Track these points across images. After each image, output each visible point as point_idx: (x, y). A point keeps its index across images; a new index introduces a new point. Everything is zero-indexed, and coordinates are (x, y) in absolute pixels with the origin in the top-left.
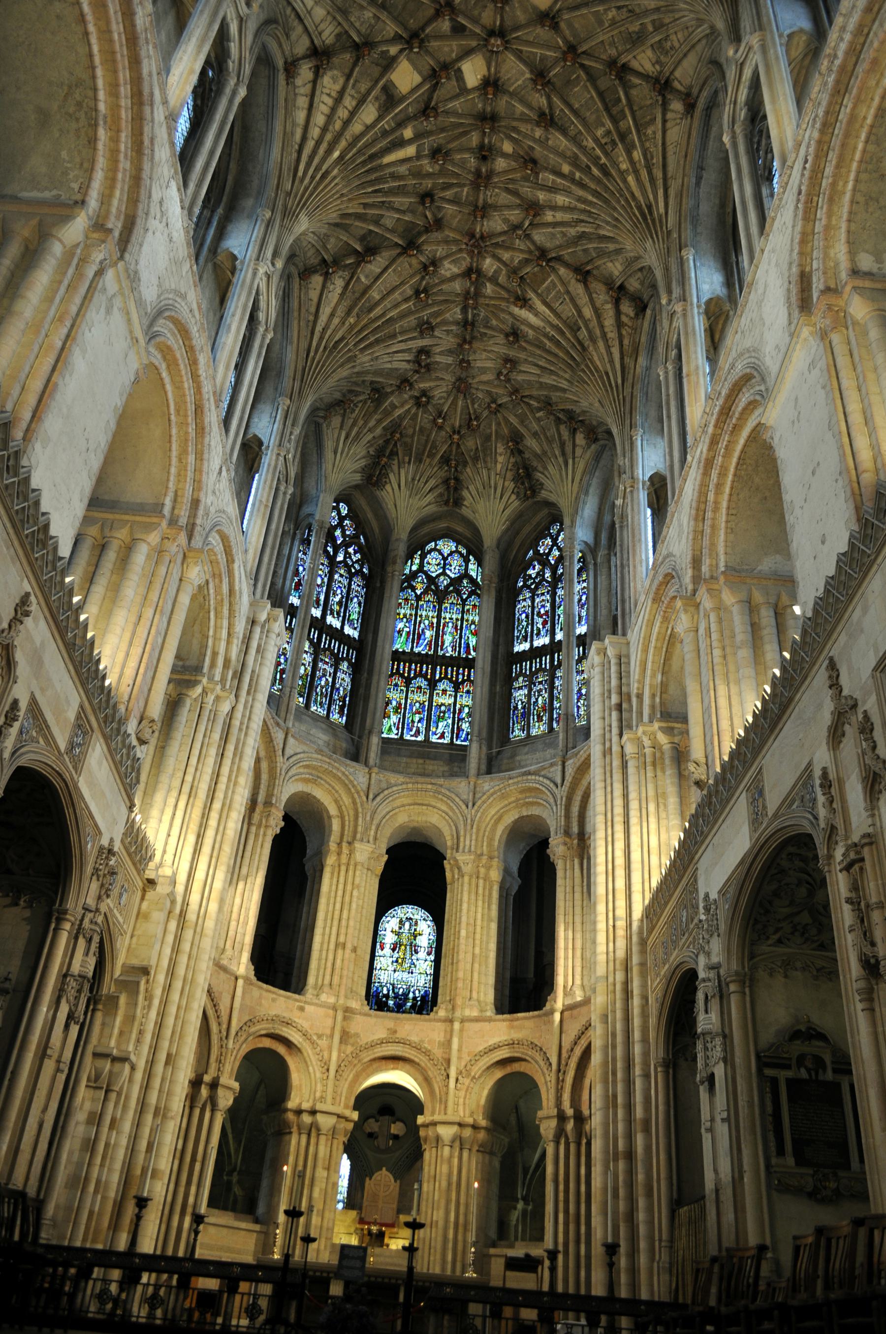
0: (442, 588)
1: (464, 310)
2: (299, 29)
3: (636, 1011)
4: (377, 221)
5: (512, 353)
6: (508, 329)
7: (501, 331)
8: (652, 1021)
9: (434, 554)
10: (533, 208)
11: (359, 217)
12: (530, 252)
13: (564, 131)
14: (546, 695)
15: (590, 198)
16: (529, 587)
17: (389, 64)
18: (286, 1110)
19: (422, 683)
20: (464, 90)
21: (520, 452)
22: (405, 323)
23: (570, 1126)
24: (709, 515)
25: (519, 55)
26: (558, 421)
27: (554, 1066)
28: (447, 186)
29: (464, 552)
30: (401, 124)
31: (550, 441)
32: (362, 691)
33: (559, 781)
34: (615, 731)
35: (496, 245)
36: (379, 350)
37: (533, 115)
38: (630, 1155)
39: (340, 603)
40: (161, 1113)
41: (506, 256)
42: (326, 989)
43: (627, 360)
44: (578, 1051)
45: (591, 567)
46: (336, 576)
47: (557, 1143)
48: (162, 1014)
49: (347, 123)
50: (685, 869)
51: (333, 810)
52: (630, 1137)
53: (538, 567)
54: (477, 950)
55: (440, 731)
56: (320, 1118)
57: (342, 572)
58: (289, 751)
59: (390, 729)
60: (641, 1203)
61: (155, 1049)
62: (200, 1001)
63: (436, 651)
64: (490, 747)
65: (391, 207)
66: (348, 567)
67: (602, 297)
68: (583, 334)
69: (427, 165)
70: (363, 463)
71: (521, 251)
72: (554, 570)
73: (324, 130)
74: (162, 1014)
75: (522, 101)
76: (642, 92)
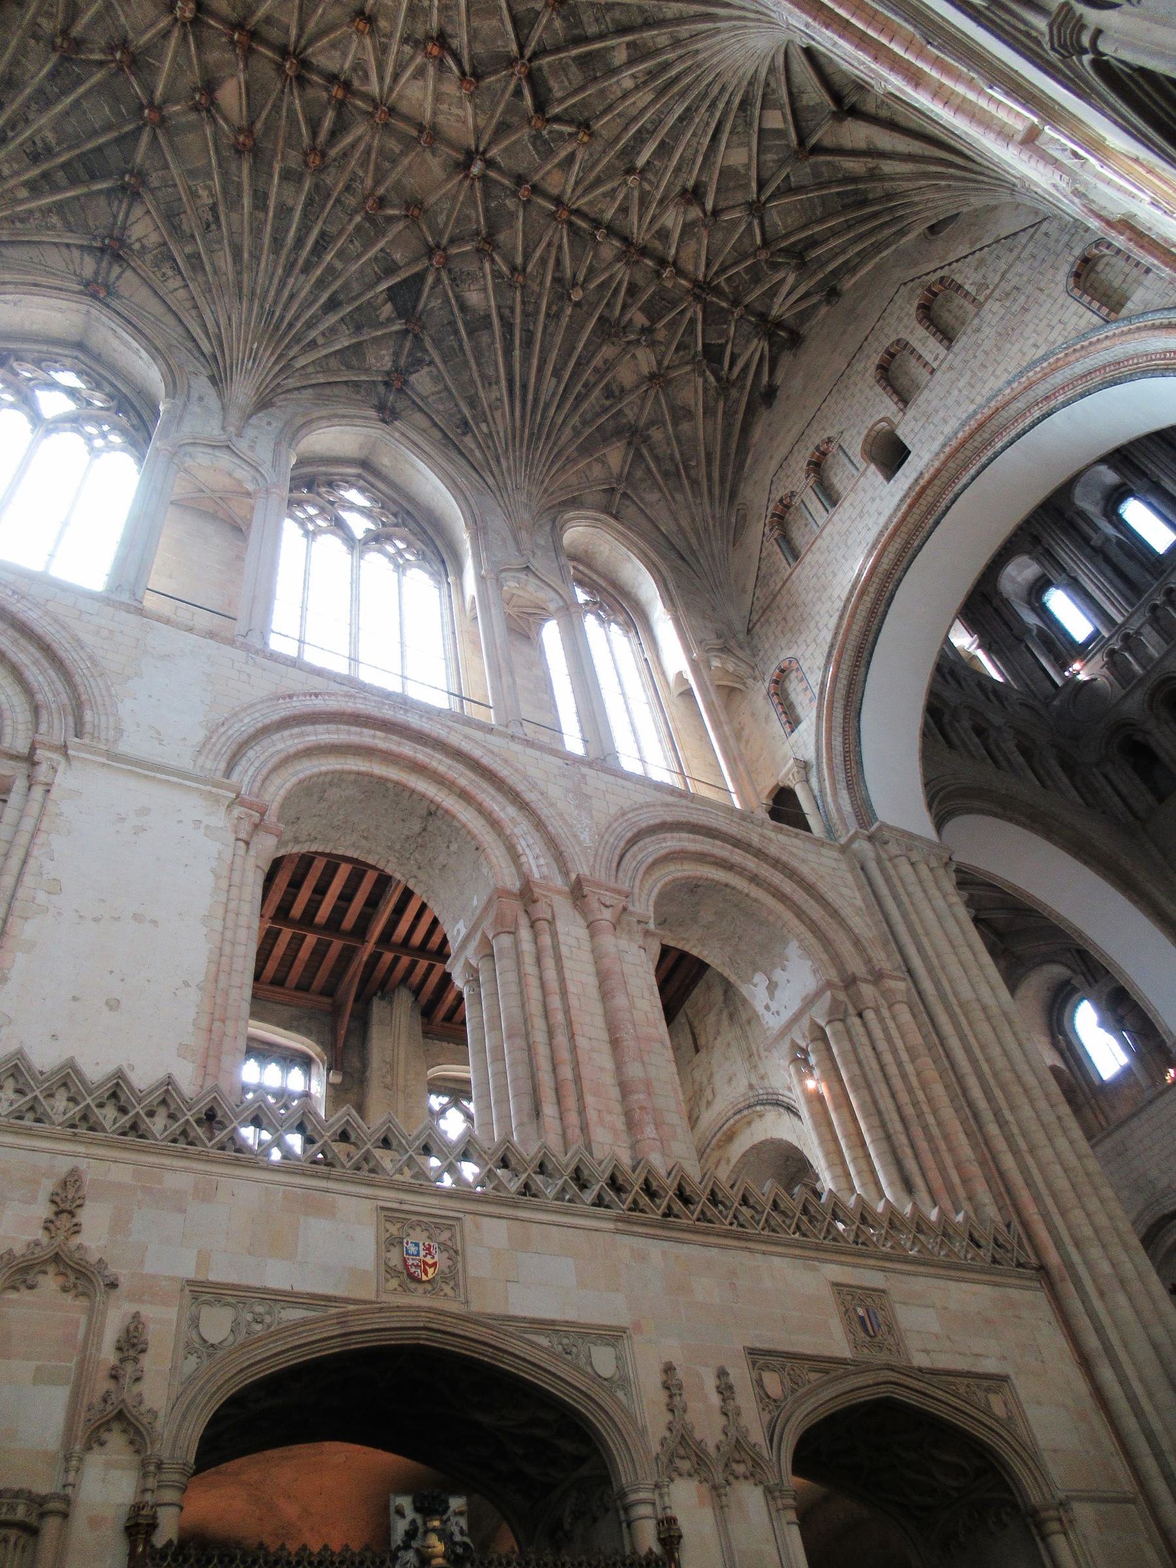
13: (53, 75)
25: (165, 35)
75: (99, 18)
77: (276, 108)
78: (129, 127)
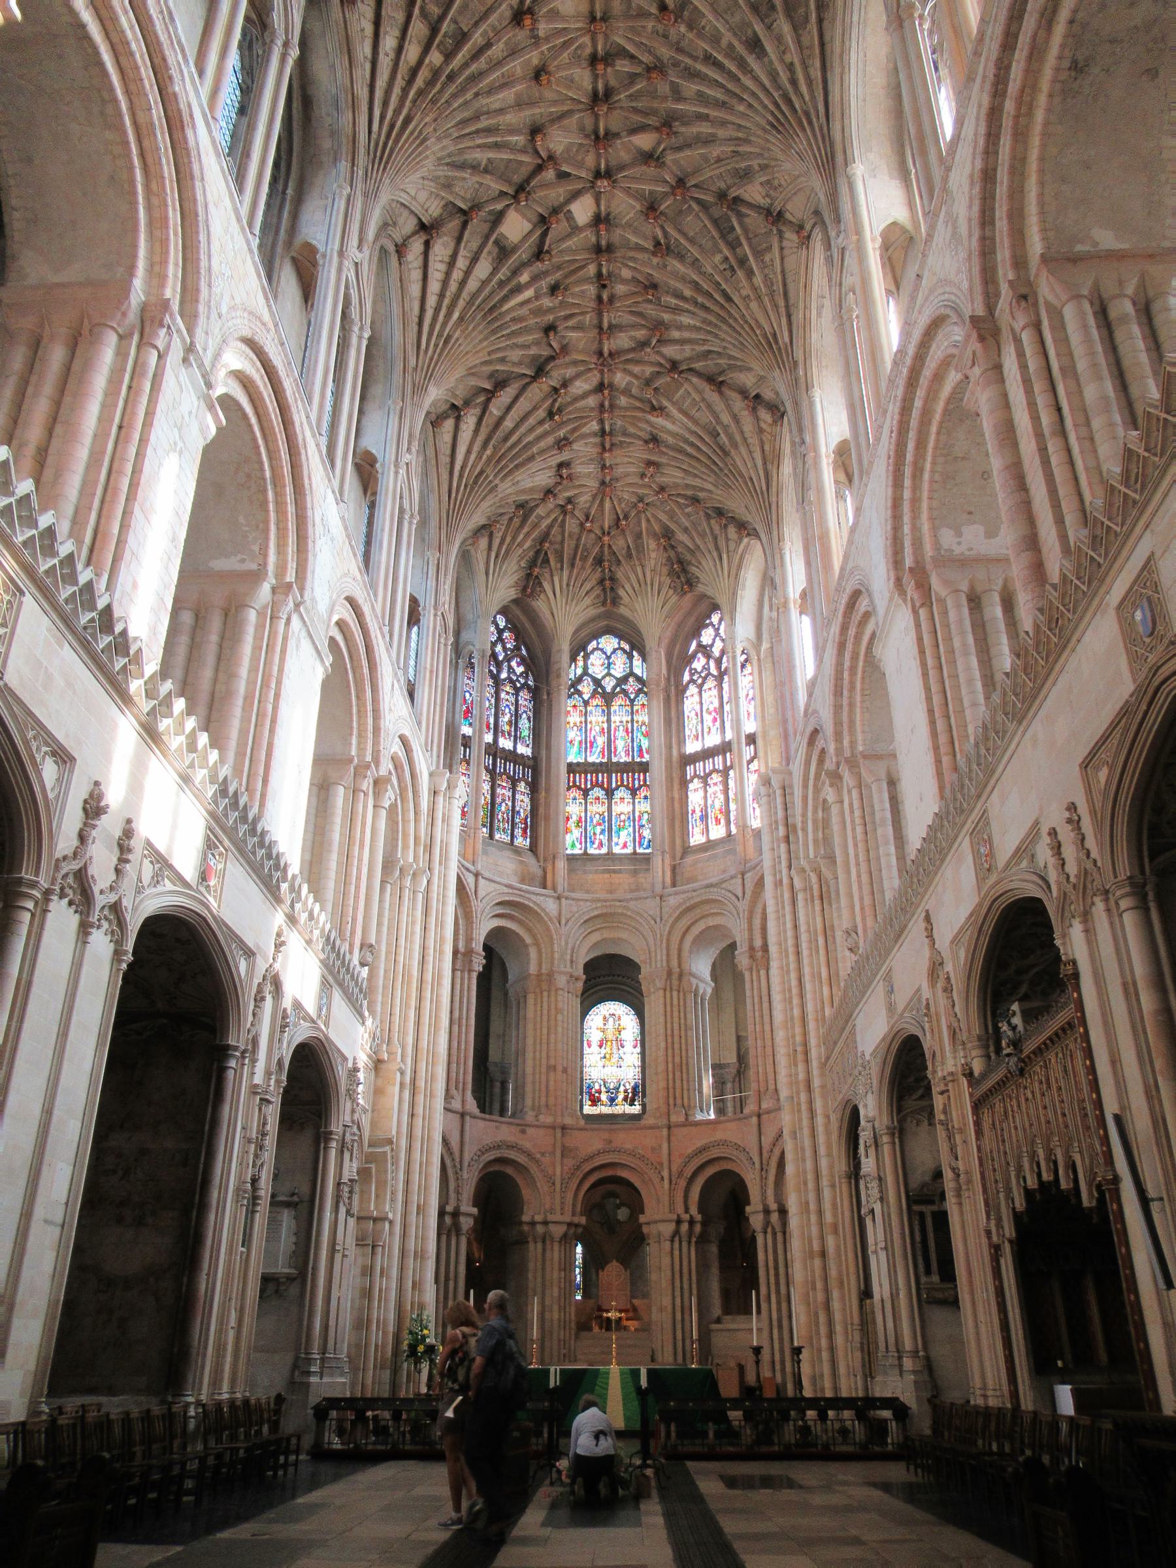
0: (609, 689)
1: (601, 421)
2: (406, 213)
3: (820, 1129)
4: (503, 360)
5: (654, 458)
6: (647, 437)
7: (639, 438)
8: (835, 1137)
9: (597, 654)
10: (658, 326)
11: (486, 363)
12: (661, 365)
13: (681, 257)
14: (722, 797)
15: (714, 320)
16: (694, 682)
17: (498, 218)
18: (521, 1223)
19: (598, 792)
20: (575, 229)
21: (673, 547)
22: (543, 444)
23: (775, 1218)
24: (845, 693)
25: (627, 190)
26: (708, 517)
27: (757, 1165)
28: (568, 317)
29: (627, 647)
30: (515, 272)
31: (703, 535)
32: (541, 810)
33: (740, 895)
34: (784, 864)
35: (628, 361)
36: (520, 475)
37: (649, 245)
38: (823, 1254)
39: (510, 723)
40: (420, 1255)
41: (637, 369)
42: (543, 1110)
43: (769, 467)
44: (777, 1152)
45: (755, 662)
46: (503, 695)
47: (765, 1233)
48: (408, 1172)
49: (463, 283)
50: (847, 1022)
51: (528, 940)
52: (822, 1238)
53: (703, 661)
54: (677, 1059)
55: (621, 842)
56: (552, 1227)
57: (508, 689)
58: (481, 893)
59: (573, 845)
60: (835, 1294)
61: (406, 1203)
62: (437, 1149)
63: (610, 758)
64: (673, 857)
65: (516, 346)
66: (511, 681)
67: (738, 404)
68: (723, 438)
69: (547, 302)
70: (515, 577)
71: (651, 364)
72: (719, 662)
73: (442, 296)
74: (408, 1172)
75: (636, 232)
76: (755, 220)
77: (636, 110)
78: (695, 206)
